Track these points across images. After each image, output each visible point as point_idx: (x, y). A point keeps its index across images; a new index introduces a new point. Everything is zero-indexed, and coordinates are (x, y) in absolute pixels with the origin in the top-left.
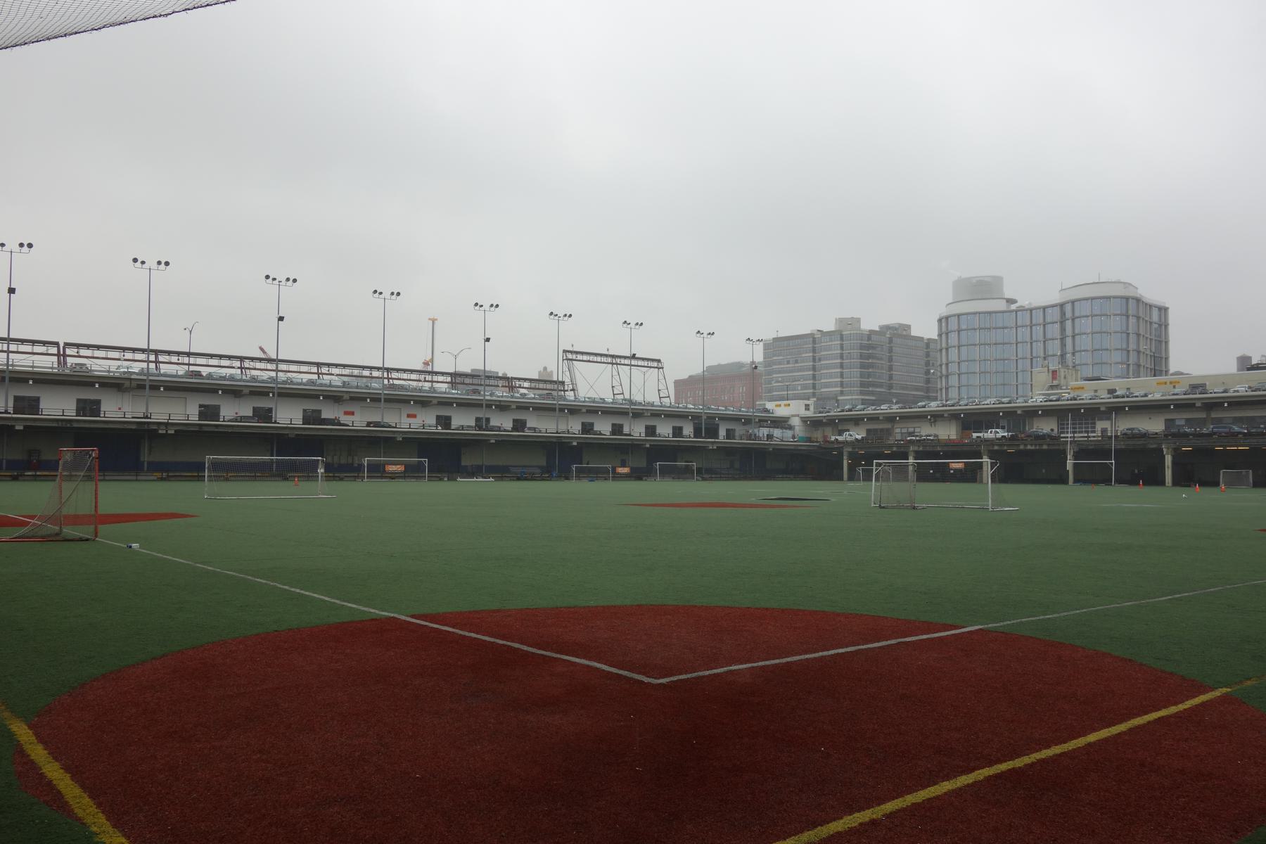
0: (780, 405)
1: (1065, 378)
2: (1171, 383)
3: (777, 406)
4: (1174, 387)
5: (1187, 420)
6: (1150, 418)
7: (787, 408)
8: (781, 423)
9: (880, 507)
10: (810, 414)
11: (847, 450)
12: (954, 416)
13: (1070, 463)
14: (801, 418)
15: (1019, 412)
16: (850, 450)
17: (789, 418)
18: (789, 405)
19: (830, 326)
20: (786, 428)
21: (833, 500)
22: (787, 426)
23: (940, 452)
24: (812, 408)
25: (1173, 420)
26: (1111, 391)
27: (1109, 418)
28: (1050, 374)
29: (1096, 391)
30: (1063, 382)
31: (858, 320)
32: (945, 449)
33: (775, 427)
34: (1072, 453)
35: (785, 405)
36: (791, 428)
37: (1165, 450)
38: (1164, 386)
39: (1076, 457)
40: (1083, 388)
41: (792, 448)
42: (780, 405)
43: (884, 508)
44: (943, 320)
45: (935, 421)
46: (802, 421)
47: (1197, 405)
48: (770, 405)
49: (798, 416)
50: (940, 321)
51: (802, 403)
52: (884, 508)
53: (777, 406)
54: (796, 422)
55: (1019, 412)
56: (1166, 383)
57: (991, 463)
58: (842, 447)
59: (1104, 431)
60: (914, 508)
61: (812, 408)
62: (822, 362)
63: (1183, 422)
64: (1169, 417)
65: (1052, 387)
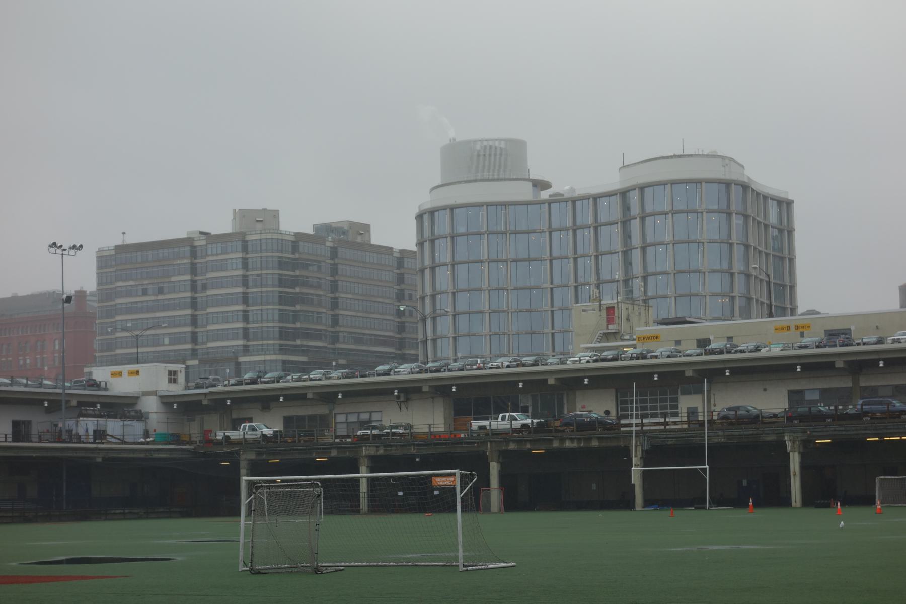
1: (628, 319)
2: (797, 328)
3: (114, 374)
4: (802, 335)
5: (823, 391)
6: (765, 390)
7: (134, 378)
9: (254, 572)
10: (178, 389)
11: (247, 456)
12: (440, 390)
13: (636, 471)
14: (161, 397)
15: (551, 381)
16: (252, 456)
17: (137, 398)
18: (137, 373)
19: (223, 225)
20: (132, 418)
21: (179, 559)
22: (133, 413)
23: (414, 456)
24: (181, 378)
25: (801, 392)
26: (703, 343)
28: (604, 313)
29: (678, 343)
30: (625, 326)
31: (275, 214)
32: (424, 451)
33: (109, 416)
34: (639, 453)
35: (131, 373)
36: (141, 416)
37: (789, 444)
38: (787, 333)
39: (647, 459)
40: (657, 337)
41: (142, 455)
43: (259, 573)
44: (426, 218)
45: (407, 400)
46: (164, 404)
47: (837, 366)
48: (100, 374)
49: (154, 393)
50: (420, 217)
51: (162, 370)
52: (259, 573)
53: (114, 374)
54: (150, 405)
55: (551, 381)
56: (788, 328)
57: (462, 476)
59: (692, 412)
60: (317, 571)
61: (181, 378)
62: (209, 293)
63: (816, 396)
64: (796, 386)
65: (607, 336)
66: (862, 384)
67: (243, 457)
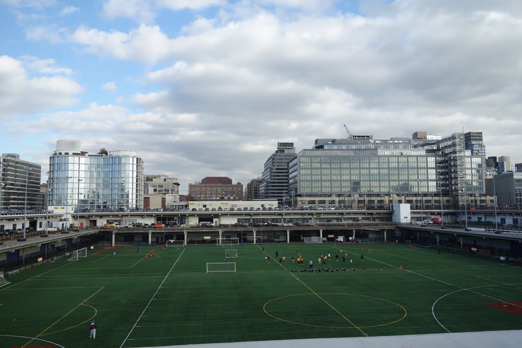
0: (58, 208)
2: (225, 204)
3: (55, 208)
4: (226, 205)
8: (59, 218)
11: (114, 232)
16: (117, 232)
27: (217, 218)
28: (173, 197)
34: (221, 233)
35: (61, 208)
37: (254, 231)
38: (223, 205)
40: (194, 204)
42: (58, 208)
44: (52, 158)
49: (69, 213)
50: (50, 158)
56: (223, 204)
58: (112, 231)
66: (253, 218)
67: (113, 232)
